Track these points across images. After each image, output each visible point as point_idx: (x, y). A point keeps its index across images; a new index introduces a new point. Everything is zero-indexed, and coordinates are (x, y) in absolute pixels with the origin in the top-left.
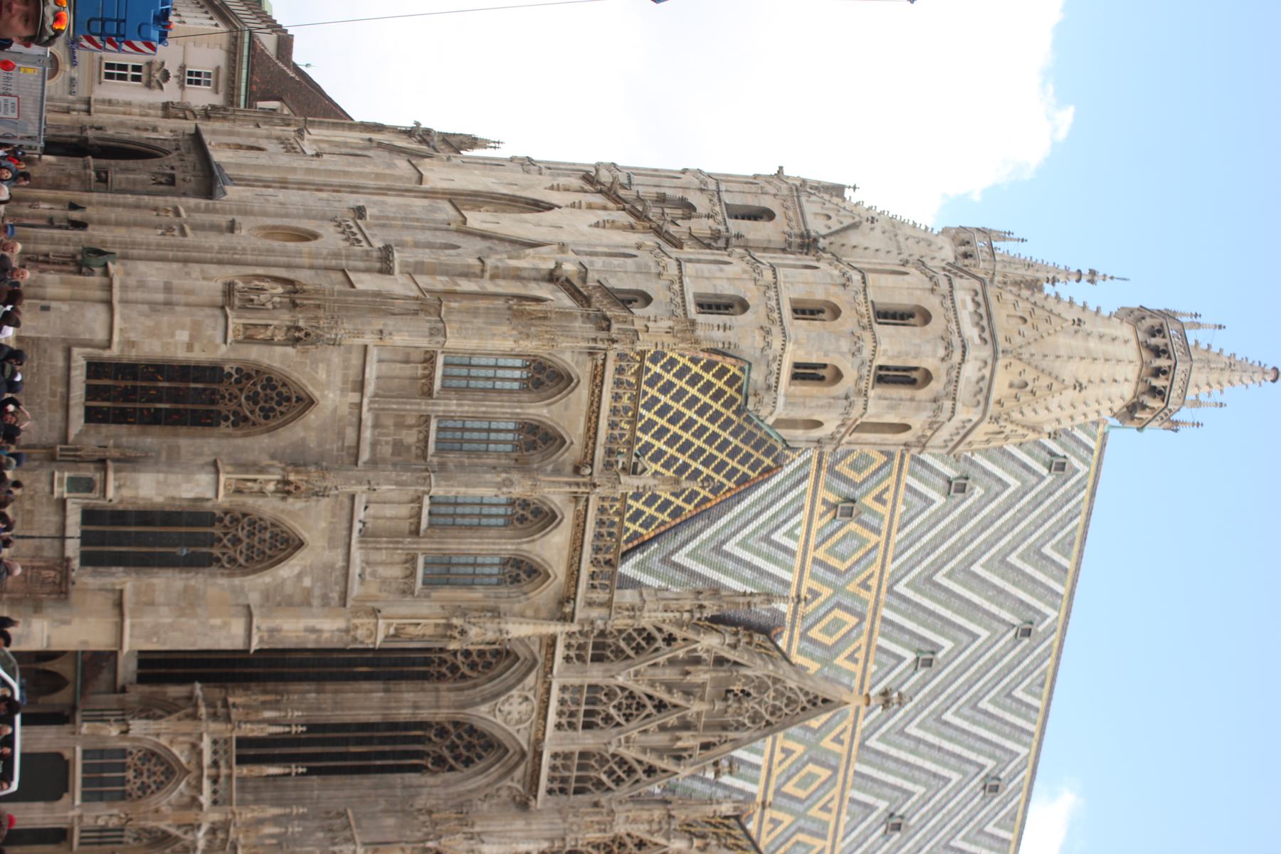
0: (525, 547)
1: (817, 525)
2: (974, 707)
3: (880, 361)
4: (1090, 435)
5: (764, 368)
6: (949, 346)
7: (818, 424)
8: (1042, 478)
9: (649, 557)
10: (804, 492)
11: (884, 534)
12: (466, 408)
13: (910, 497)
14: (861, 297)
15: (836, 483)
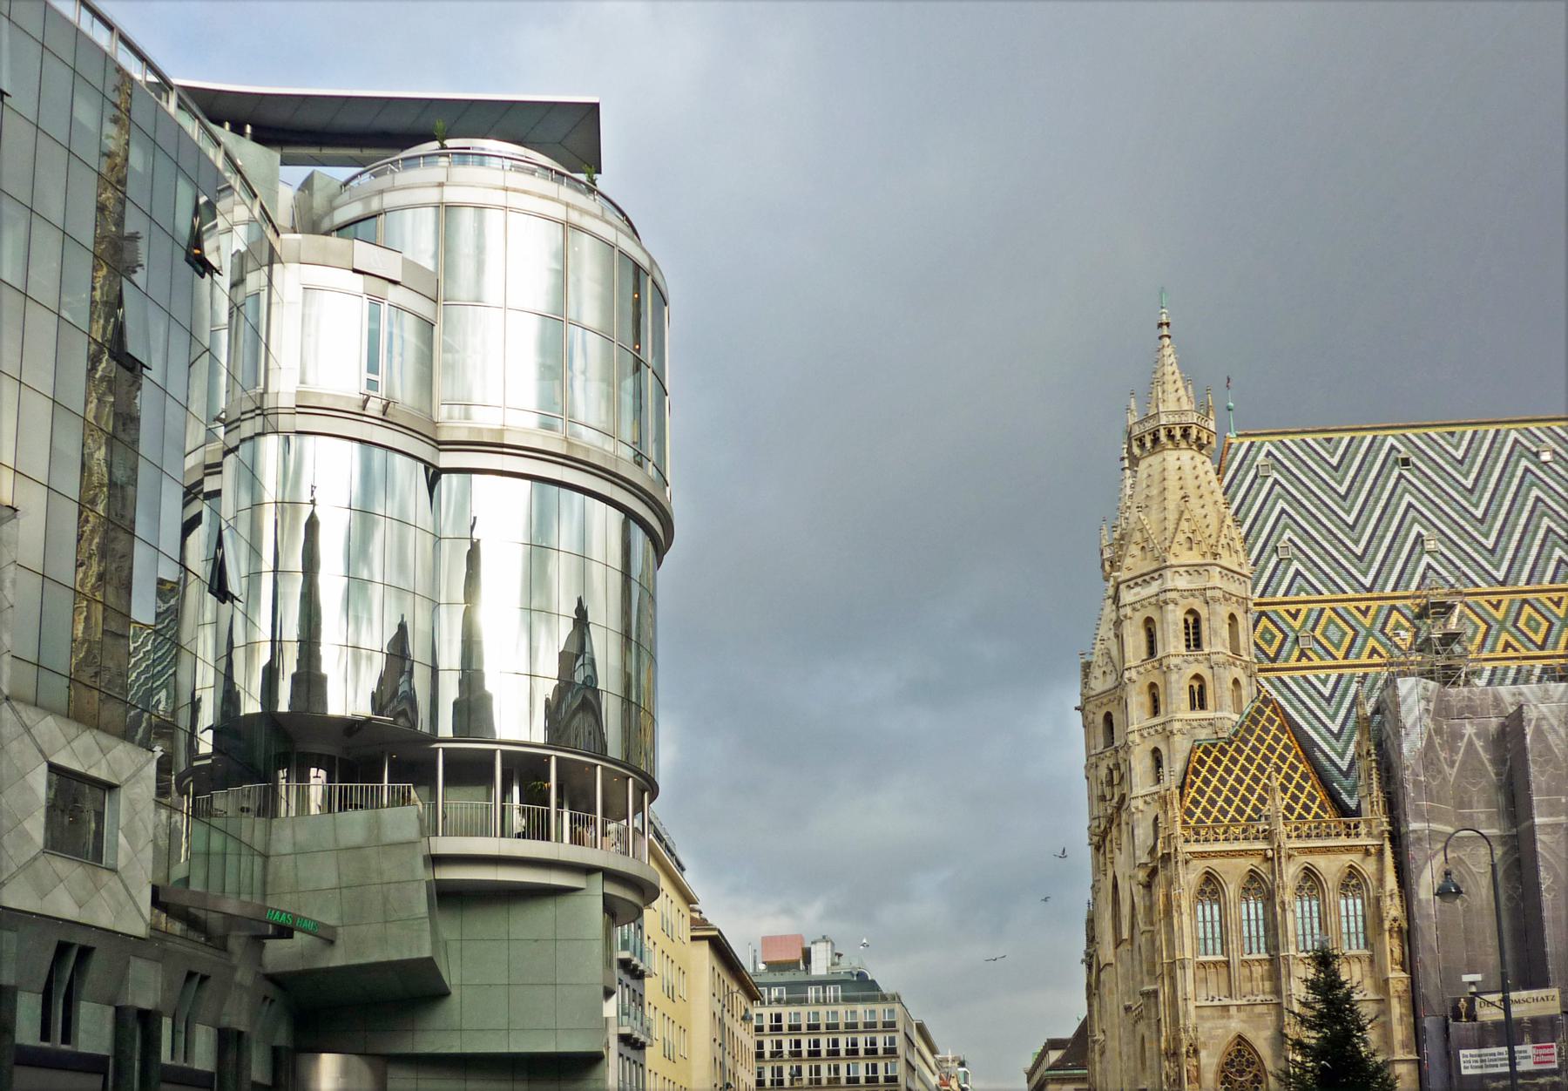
0: (1330, 885)
1: (1317, 662)
2: (1471, 491)
3: (1183, 649)
4: (1238, 450)
5: (1196, 731)
6: (1166, 602)
7: (1236, 682)
8: (1276, 482)
9: (1345, 789)
10: (1291, 678)
11: (1323, 605)
12: (1234, 938)
13: (1294, 590)
14: (1142, 670)
15: (1284, 653)
